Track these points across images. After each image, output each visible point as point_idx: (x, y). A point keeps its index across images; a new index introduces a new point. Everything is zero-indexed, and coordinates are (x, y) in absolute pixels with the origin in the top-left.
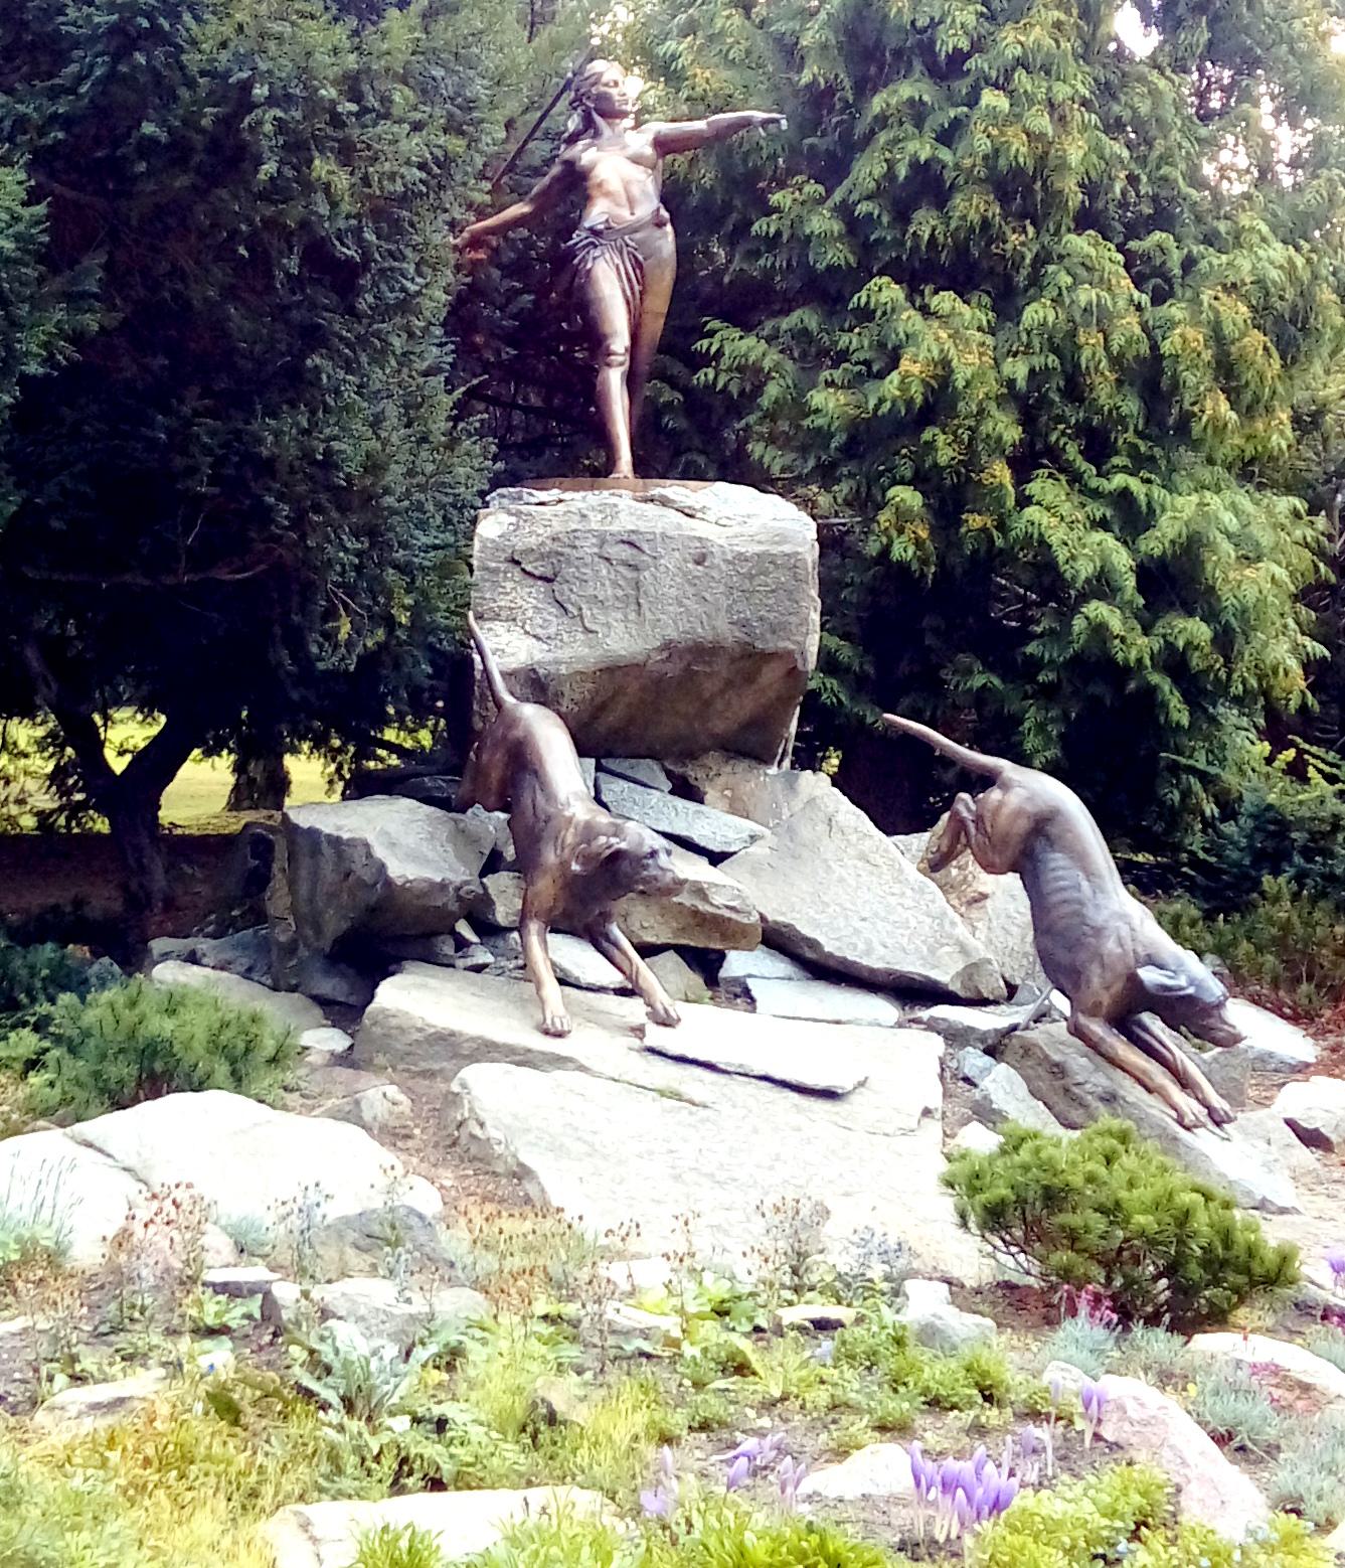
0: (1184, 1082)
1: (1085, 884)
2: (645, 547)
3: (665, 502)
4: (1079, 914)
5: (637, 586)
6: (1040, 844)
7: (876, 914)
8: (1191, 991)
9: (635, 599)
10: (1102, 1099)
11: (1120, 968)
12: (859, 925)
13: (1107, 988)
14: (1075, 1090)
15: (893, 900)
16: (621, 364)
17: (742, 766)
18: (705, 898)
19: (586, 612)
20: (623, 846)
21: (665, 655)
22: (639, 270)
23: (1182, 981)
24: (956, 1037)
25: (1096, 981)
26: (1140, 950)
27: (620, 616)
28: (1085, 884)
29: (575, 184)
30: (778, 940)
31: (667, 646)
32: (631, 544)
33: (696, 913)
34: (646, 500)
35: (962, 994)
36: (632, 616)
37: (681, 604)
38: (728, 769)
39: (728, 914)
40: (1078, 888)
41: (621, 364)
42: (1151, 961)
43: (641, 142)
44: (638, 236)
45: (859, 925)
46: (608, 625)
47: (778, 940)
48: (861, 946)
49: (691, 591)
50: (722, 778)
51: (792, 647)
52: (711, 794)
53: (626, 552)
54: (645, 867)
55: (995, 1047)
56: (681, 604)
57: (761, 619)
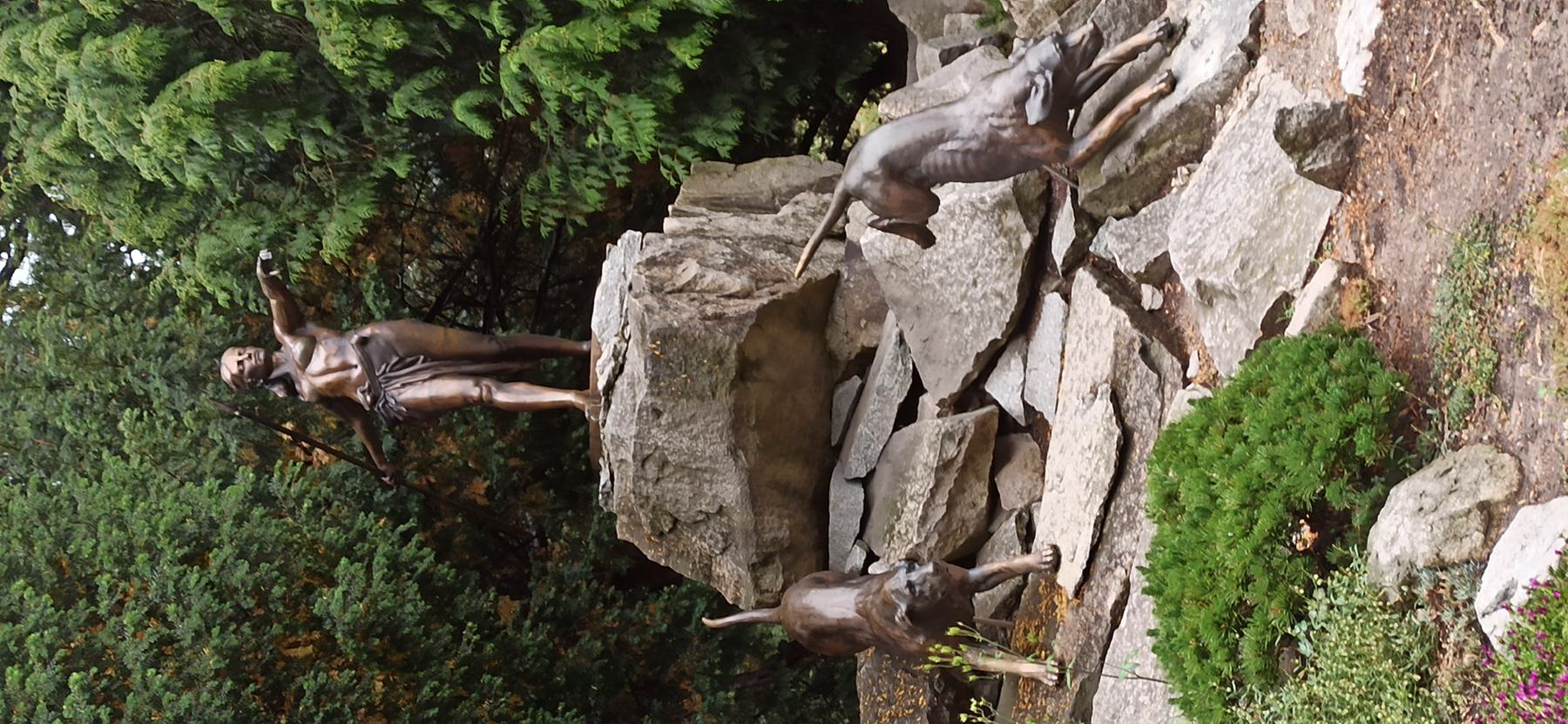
0: (1132, 54)
1: (950, 145)
2: (647, 452)
3: (610, 387)
4: (977, 154)
5: (681, 467)
6: (914, 175)
7: (972, 267)
8: (1049, 75)
9: (692, 472)
10: (1142, 153)
11: (1026, 132)
12: (978, 292)
13: (1043, 143)
14: (1132, 172)
15: (959, 245)
16: (489, 391)
17: (840, 308)
18: (952, 461)
19: (704, 508)
20: (903, 607)
21: (740, 452)
22: (408, 358)
23: (1040, 81)
24: (1079, 255)
25: (1038, 150)
26: (1010, 112)
27: (706, 486)
28: (950, 145)
29: (334, 398)
30: (989, 361)
31: (733, 452)
32: (644, 461)
33: (964, 467)
34: (608, 403)
35: (1042, 213)
36: (707, 476)
37: (695, 438)
38: (842, 322)
39: (964, 446)
40: (953, 152)
41: (489, 391)
42: (1021, 100)
43: (294, 347)
44: (376, 361)
45: (978, 292)
46: (715, 496)
47: (989, 361)
48: (998, 302)
49: (685, 427)
50: (847, 339)
51: (735, 347)
52: (864, 340)
53: (651, 470)
54: (921, 592)
55: (1089, 223)
56: (695, 438)
57: (710, 372)
